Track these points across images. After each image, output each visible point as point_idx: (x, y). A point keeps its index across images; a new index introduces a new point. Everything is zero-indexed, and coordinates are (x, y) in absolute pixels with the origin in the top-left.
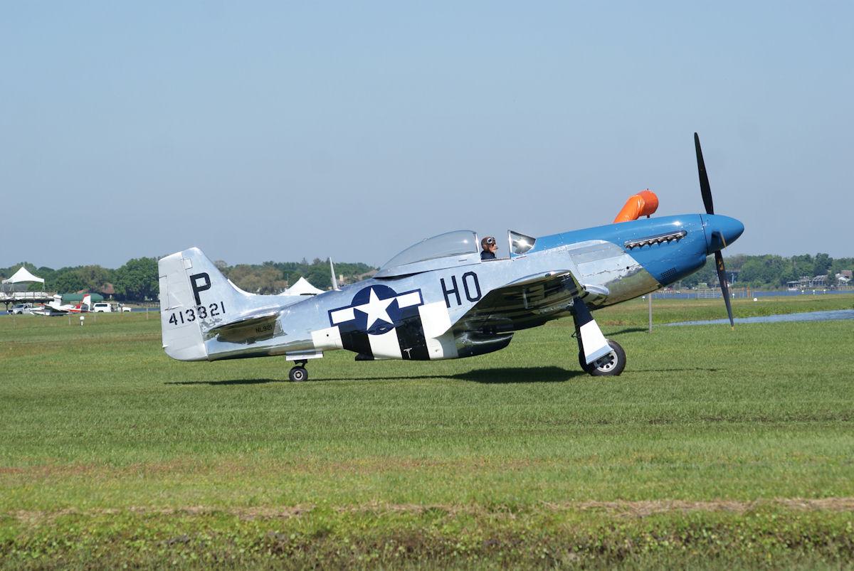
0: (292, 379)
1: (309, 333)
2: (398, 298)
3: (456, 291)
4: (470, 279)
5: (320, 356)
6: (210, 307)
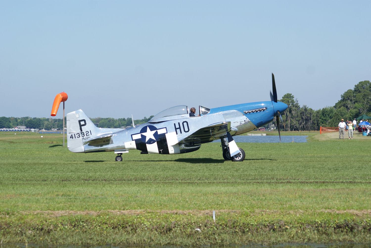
0: (116, 160)
1: (124, 143)
2: (158, 131)
3: (180, 128)
4: (185, 124)
5: (127, 152)
6: (86, 132)
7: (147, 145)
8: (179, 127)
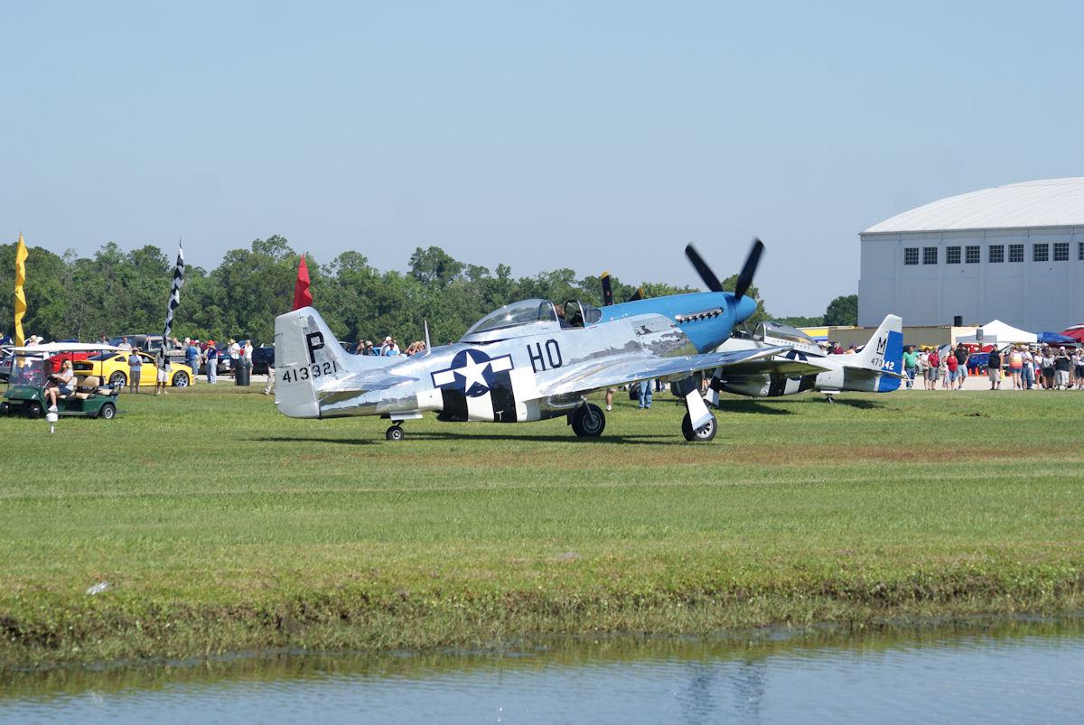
2: (491, 362)
3: (540, 357)
4: (552, 346)
5: (419, 416)
7: (469, 399)
8: (537, 354)
